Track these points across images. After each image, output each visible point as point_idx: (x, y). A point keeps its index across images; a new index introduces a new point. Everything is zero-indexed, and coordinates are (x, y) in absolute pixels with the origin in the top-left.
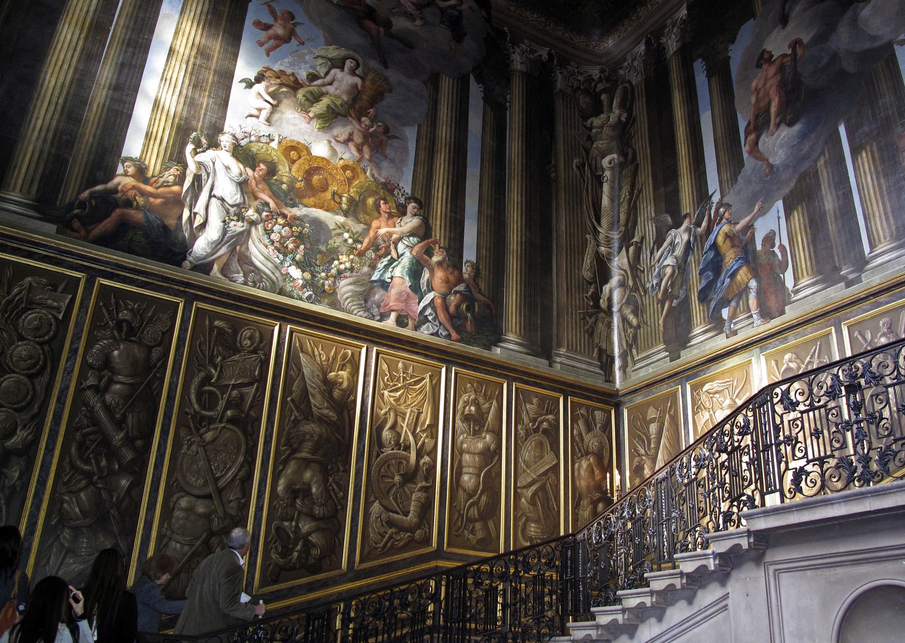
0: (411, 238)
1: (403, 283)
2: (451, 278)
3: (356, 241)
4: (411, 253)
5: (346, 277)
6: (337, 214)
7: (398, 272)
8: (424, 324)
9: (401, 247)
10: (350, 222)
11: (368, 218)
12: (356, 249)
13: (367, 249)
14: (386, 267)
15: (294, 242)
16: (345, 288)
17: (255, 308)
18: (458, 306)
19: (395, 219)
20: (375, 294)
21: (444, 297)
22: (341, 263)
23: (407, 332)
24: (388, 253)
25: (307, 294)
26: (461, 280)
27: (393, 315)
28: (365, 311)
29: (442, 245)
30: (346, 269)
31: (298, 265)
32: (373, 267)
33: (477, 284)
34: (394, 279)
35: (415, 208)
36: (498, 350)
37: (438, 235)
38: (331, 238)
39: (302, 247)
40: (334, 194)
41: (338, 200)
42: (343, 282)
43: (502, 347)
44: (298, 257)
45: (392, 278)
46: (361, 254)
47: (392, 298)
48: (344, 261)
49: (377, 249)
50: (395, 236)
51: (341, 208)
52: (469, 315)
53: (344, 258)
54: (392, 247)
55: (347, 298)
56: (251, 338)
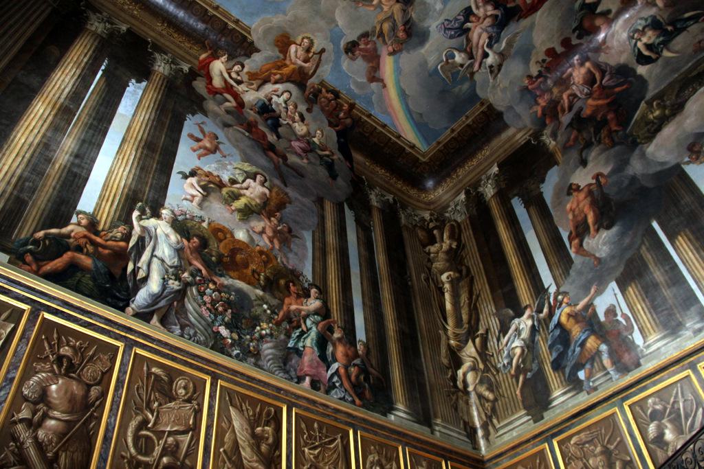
0: (316, 317)
1: (313, 352)
2: (350, 353)
3: (273, 312)
4: (317, 328)
5: (267, 342)
6: (257, 288)
7: (308, 342)
8: (333, 389)
9: (309, 322)
10: (268, 297)
11: (281, 295)
12: (274, 319)
13: (282, 320)
14: (299, 337)
15: (222, 305)
16: (267, 349)
17: (189, 360)
18: (357, 377)
19: (302, 299)
20: (291, 360)
21: (346, 367)
22: (262, 329)
23: (319, 397)
24: (299, 326)
25: (236, 352)
26: (356, 355)
27: (308, 379)
28: (285, 373)
29: (340, 325)
30: (266, 334)
31: (227, 326)
32: (289, 337)
33: (369, 360)
34: (306, 348)
35: (316, 293)
36: (392, 417)
37: (335, 315)
38: (253, 307)
39: (230, 311)
40: (254, 271)
41: (256, 276)
42: (265, 346)
43: (395, 415)
44: (226, 319)
45: (304, 347)
46: (278, 324)
47: (306, 364)
48: (264, 328)
49: (290, 322)
50: (303, 313)
51: (260, 283)
52: (367, 385)
53: (264, 325)
54: (302, 321)
55: (269, 360)
56: (185, 388)
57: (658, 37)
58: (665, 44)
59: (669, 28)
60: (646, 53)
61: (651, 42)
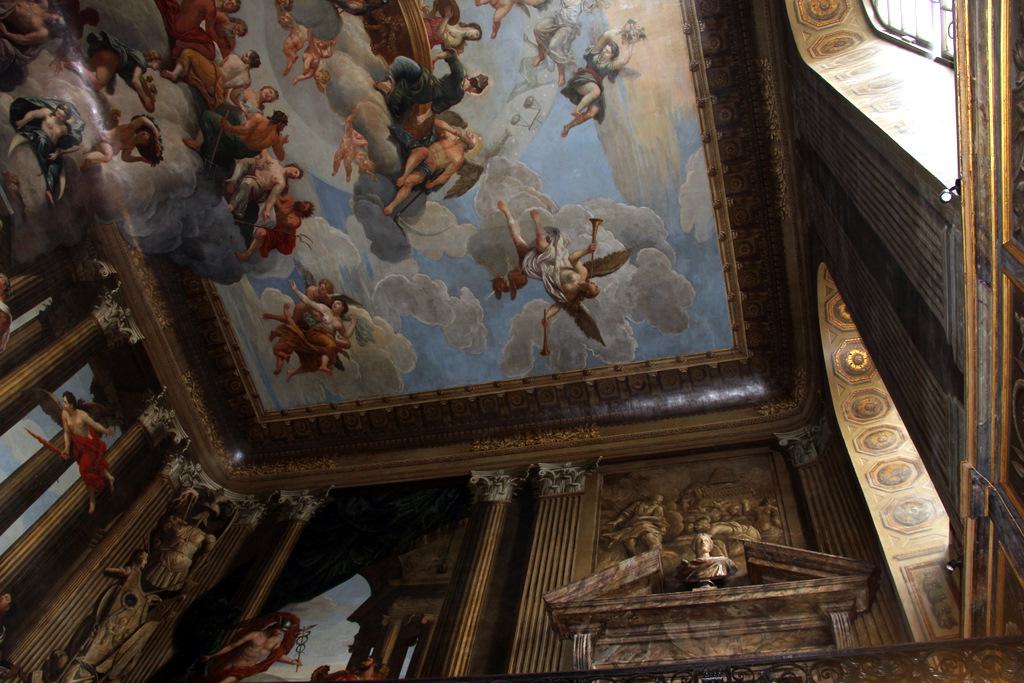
57: (47, 138)
58: (34, 144)
59: (54, 156)
60: (29, 115)
61: (44, 126)
